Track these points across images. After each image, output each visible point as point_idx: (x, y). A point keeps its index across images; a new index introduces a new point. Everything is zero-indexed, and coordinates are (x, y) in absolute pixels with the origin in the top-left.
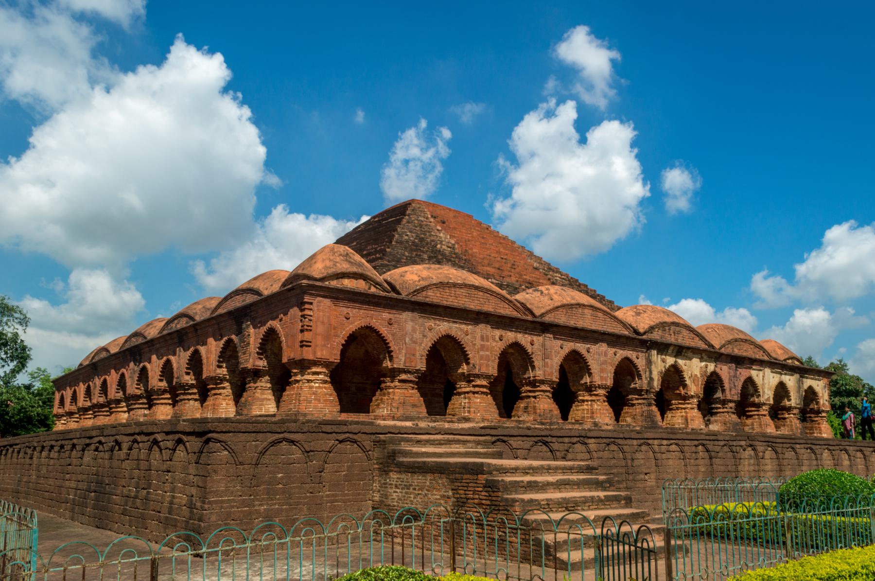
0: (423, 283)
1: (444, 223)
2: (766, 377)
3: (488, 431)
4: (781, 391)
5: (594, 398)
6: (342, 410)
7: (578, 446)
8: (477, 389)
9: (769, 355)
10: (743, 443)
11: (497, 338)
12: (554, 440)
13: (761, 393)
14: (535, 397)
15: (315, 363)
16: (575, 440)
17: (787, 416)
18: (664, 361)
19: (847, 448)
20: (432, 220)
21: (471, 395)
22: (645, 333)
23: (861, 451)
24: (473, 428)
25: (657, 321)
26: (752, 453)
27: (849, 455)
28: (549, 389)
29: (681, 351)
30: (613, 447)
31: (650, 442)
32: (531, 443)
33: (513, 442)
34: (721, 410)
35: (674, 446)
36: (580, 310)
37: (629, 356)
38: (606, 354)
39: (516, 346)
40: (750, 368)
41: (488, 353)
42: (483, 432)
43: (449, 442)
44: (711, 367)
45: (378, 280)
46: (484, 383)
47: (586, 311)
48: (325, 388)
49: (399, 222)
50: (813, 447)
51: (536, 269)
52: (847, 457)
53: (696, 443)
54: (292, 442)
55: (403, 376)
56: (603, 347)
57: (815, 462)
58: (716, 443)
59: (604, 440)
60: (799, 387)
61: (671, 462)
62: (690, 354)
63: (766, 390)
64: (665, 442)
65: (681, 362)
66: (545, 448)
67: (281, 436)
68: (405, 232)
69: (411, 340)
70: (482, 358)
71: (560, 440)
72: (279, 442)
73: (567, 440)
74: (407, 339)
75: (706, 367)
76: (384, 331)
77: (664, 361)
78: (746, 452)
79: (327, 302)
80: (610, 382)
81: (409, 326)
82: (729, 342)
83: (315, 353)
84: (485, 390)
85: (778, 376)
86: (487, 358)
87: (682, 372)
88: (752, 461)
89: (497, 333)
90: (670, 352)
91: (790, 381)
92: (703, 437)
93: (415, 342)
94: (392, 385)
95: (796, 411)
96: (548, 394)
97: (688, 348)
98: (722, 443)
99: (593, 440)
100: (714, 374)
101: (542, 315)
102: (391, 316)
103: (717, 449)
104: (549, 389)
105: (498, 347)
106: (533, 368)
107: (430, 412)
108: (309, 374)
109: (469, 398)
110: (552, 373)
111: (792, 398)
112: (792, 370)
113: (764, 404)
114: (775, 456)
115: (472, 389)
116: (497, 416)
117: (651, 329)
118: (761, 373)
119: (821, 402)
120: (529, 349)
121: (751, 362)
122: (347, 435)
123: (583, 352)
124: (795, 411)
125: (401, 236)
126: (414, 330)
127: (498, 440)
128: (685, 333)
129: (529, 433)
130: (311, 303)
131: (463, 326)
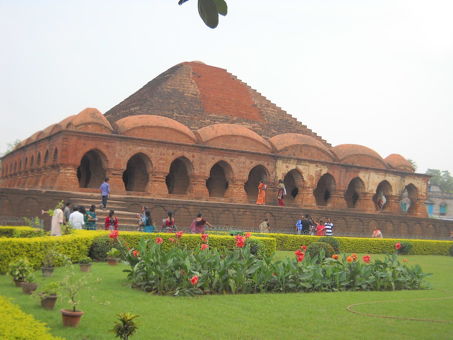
0: (134, 126)
1: (199, 77)
2: (371, 177)
3: (129, 200)
4: (383, 186)
7: (183, 210)
8: (157, 179)
11: (171, 154)
12: (167, 205)
13: (366, 187)
14: (195, 184)
15: (68, 165)
16: (181, 206)
17: (391, 201)
19: (393, 220)
20: (191, 76)
22: (281, 151)
23: (405, 222)
24: (121, 198)
27: (393, 225)
28: (203, 180)
29: (299, 161)
31: (230, 209)
32: (153, 206)
35: (248, 212)
36: (234, 138)
37: (261, 164)
38: (244, 163)
39: (183, 157)
41: (164, 162)
42: (126, 200)
44: (325, 171)
45: (107, 126)
46: (162, 176)
48: (73, 176)
49: (167, 78)
51: (255, 106)
52: (391, 225)
53: (265, 211)
54: (34, 199)
55: (115, 172)
56: (242, 159)
57: (361, 227)
58: (281, 212)
59: (200, 207)
62: (308, 164)
63: (370, 185)
64: (242, 210)
65: (301, 167)
66: (162, 208)
67: (29, 196)
68: (167, 87)
69: (119, 155)
70: (160, 164)
71: (171, 206)
72: (28, 198)
73: (175, 206)
74: (117, 155)
75: (321, 170)
76: (104, 151)
77: (287, 167)
79: (75, 138)
80: (246, 177)
81: (118, 147)
82: (350, 156)
84: (161, 180)
85: (383, 177)
86: (163, 164)
89: (171, 152)
91: (392, 180)
92: (270, 209)
93: (121, 156)
96: (202, 183)
97: (305, 160)
98: (285, 213)
99: (192, 207)
100: (327, 175)
101: (207, 142)
102: (109, 144)
103: (281, 215)
104: (203, 180)
105: (171, 159)
107: (127, 189)
108: (66, 170)
110: (205, 173)
111: (393, 190)
112: (396, 173)
113: (367, 193)
115: (154, 179)
116: (167, 193)
117: (286, 149)
118: (367, 176)
119: (420, 193)
120: (191, 159)
121: (360, 168)
125: (163, 89)
127: (135, 204)
128: (314, 150)
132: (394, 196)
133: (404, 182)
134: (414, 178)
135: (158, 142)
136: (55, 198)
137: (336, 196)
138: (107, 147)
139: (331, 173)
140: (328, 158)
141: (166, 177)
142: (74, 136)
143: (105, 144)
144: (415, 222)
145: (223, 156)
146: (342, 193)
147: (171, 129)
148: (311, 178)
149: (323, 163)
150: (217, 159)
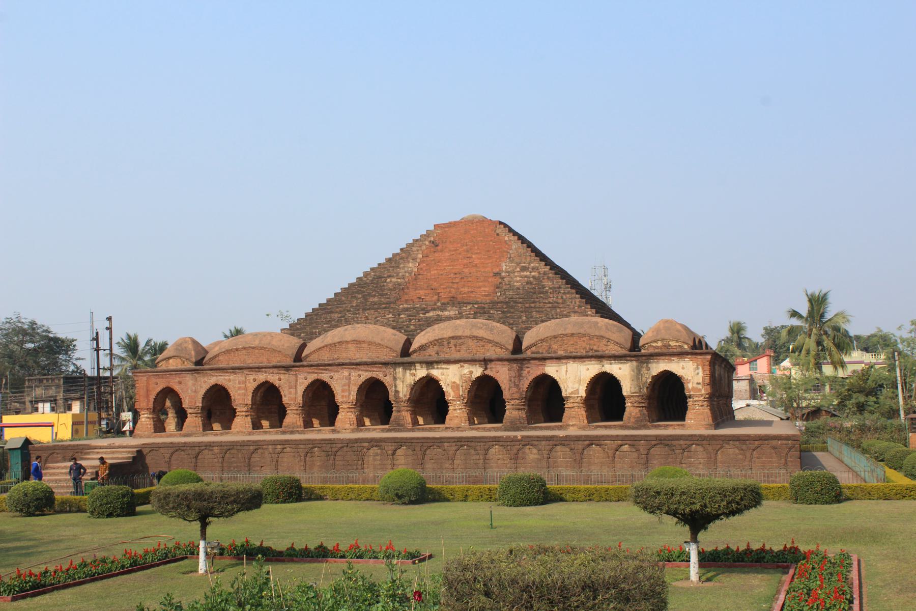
6: (156, 431)
9: (616, 343)
10: (366, 444)
18: (414, 375)
22: (415, 351)
25: (431, 339)
26: (379, 451)
29: (430, 364)
30: (232, 451)
33: (162, 451)
43: (113, 452)
44: (477, 372)
47: (350, 345)
50: (473, 444)
52: (535, 451)
60: (638, 374)
61: (285, 459)
63: (570, 385)
64: (279, 447)
65: (436, 373)
66: (183, 453)
70: (239, 395)
75: (471, 373)
76: (177, 388)
78: (371, 451)
82: (543, 340)
88: (378, 458)
89: (251, 378)
90: (418, 366)
98: (340, 445)
105: (252, 386)
110: (296, 398)
114: (410, 452)
116: (251, 429)
118: (563, 368)
119: (690, 386)
120: (277, 384)
121: (545, 359)
124: (632, 399)
128: (471, 343)
131: (227, 378)
132: (629, 396)
133: (648, 369)
134: (671, 361)
135: (233, 369)
138: (180, 383)
139: (488, 372)
140: (498, 350)
143: (177, 380)
144: (587, 442)
146: (517, 402)
147: (261, 348)
148: (455, 386)
149: (472, 361)
150: (312, 377)
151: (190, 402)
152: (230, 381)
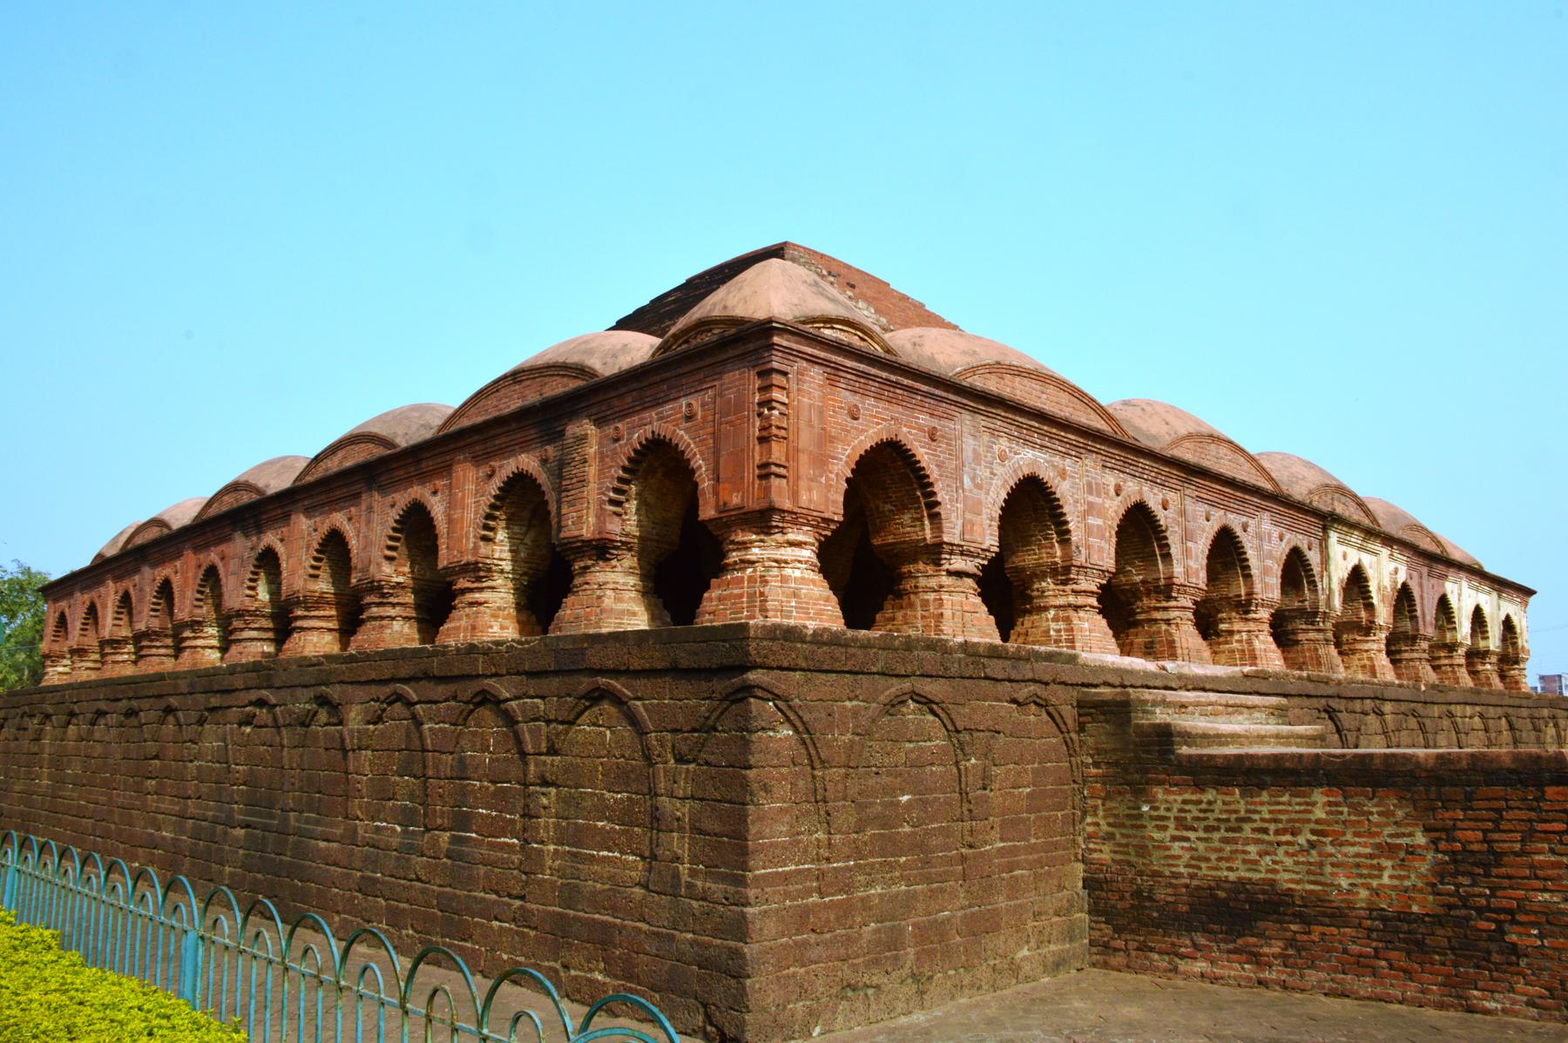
5: (1252, 626)
8: (1081, 600)
14: (1168, 622)
17: (1480, 668)
18: (1345, 557)
21: (1071, 613)
34: (1406, 655)
40: (1444, 577)
42: (1248, 685)
54: (927, 703)
55: (958, 563)
65: (1367, 560)
67: (906, 685)
69: (973, 480)
74: (967, 480)
77: (1345, 557)
79: (816, 374)
81: (969, 444)
83: (795, 495)
87: (1366, 580)
91: (1488, 601)
94: (933, 583)
95: (1494, 659)
100: (1404, 585)
102: (935, 423)
106: (1167, 557)
108: (779, 546)
109: (1067, 620)
115: (1072, 599)
122: (1032, 687)
123: (1238, 531)
126: (977, 457)
129: (1310, 688)
130: (785, 374)
131: (1057, 459)
136: (1024, 692)
137: (1416, 655)
141: (1101, 587)
142: (813, 360)
143: (923, 419)
145: (1227, 509)
150: (1219, 518)
151: (967, 526)
152: (1063, 474)
